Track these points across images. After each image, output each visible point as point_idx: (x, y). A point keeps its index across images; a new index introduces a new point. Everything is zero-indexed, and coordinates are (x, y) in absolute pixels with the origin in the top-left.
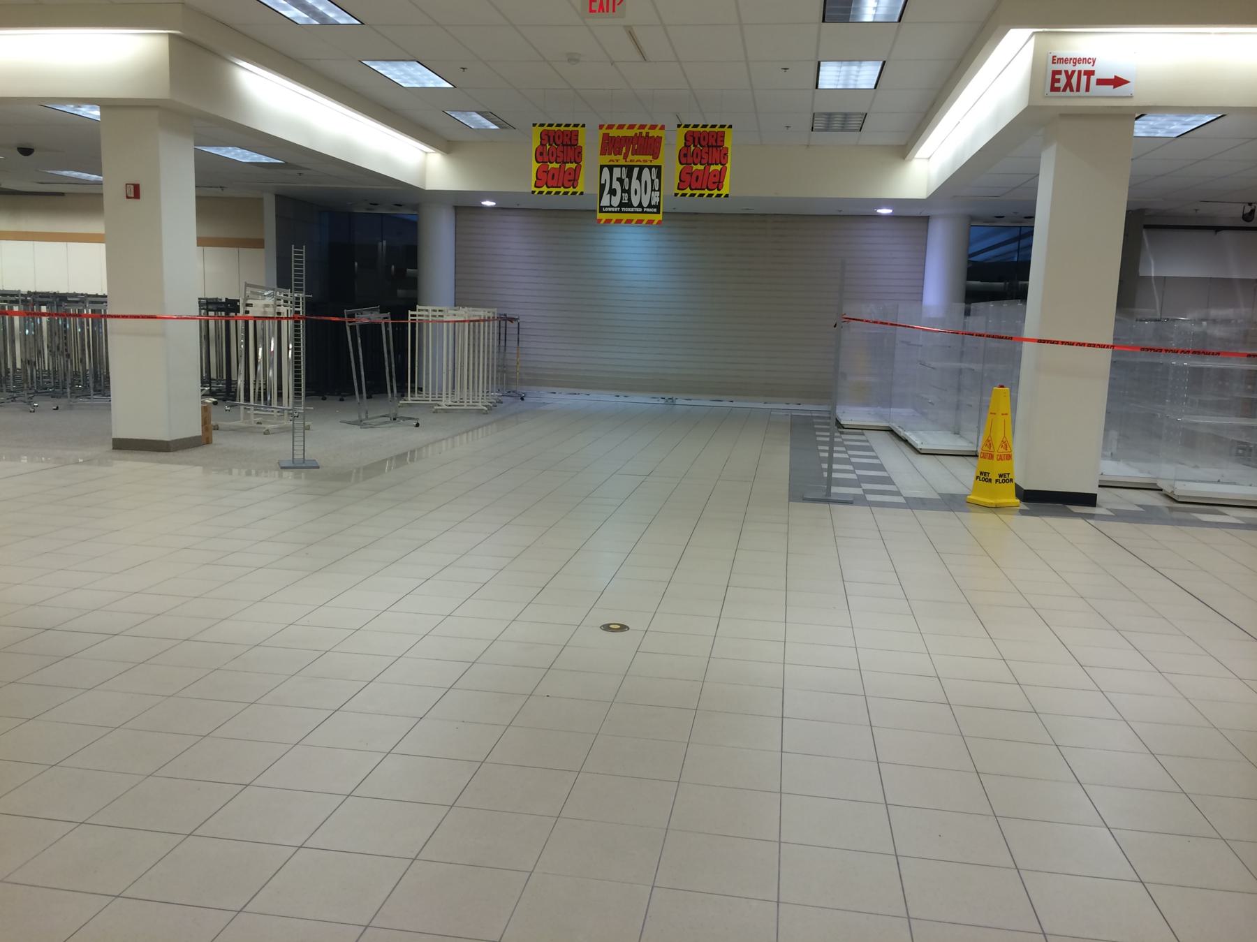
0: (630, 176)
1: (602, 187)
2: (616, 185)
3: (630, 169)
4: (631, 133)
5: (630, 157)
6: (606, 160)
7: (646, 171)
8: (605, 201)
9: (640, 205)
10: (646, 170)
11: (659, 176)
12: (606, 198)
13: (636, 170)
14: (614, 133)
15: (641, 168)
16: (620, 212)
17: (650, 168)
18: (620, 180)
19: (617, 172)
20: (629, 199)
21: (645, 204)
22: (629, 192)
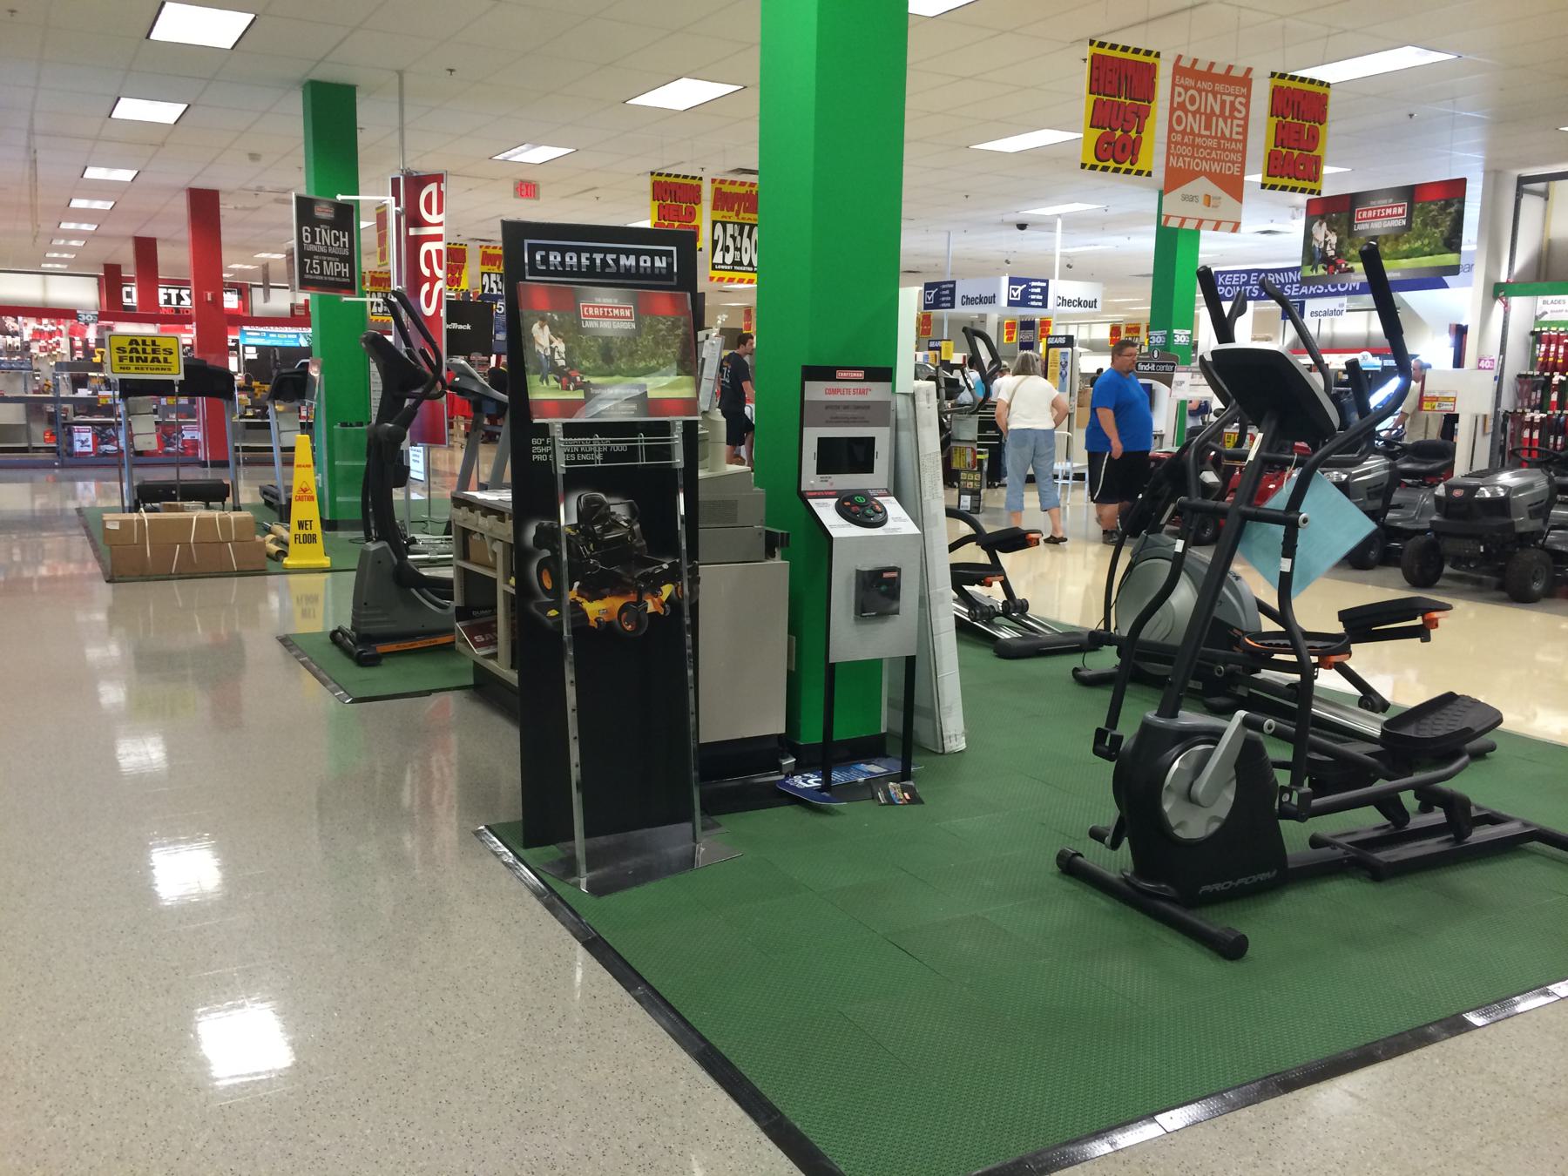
0: (741, 234)
1: (715, 243)
2: (730, 242)
3: (742, 226)
4: (742, 190)
5: (742, 215)
6: (719, 215)
8: (718, 258)
9: (750, 264)
14: (726, 188)
15: (752, 226)
18: (733, 236)
19: (730, 227)
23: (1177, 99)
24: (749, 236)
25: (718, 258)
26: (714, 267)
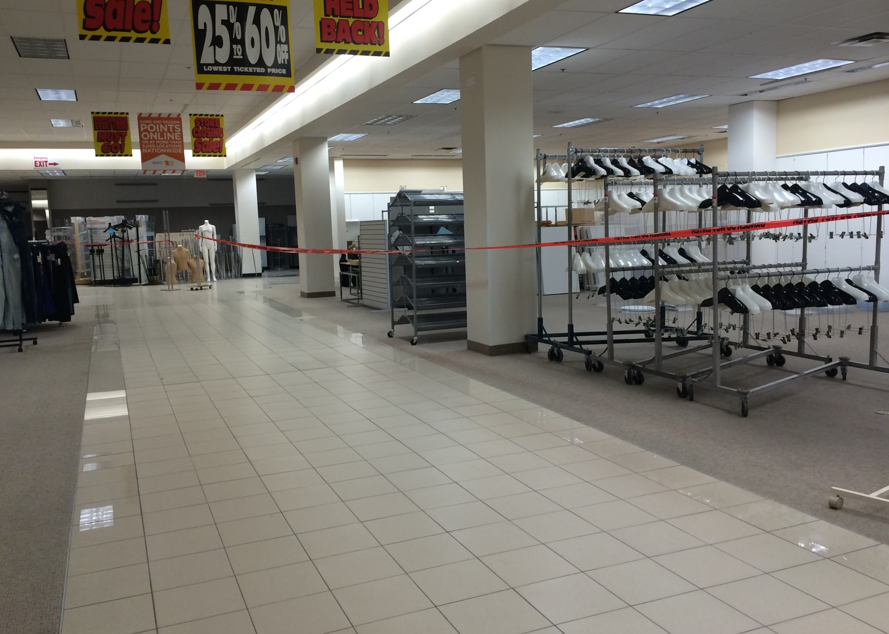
0: (242, 18)
1: (199, 36)
2: (222, 31)
7: (265, 12)
10: (265, 12)
11: (284, 21)
12: (207, 50)
13: (252, 10)
15: (260, 8)
16: (232, 72)
17: (271, 8)
18: (226, 23)
20: (244, 53)
21: (269, 62)
22: (242, 42)
23: (142, 129)
24: (257, 21)
25: (207, 57)
26: (201, 69)
